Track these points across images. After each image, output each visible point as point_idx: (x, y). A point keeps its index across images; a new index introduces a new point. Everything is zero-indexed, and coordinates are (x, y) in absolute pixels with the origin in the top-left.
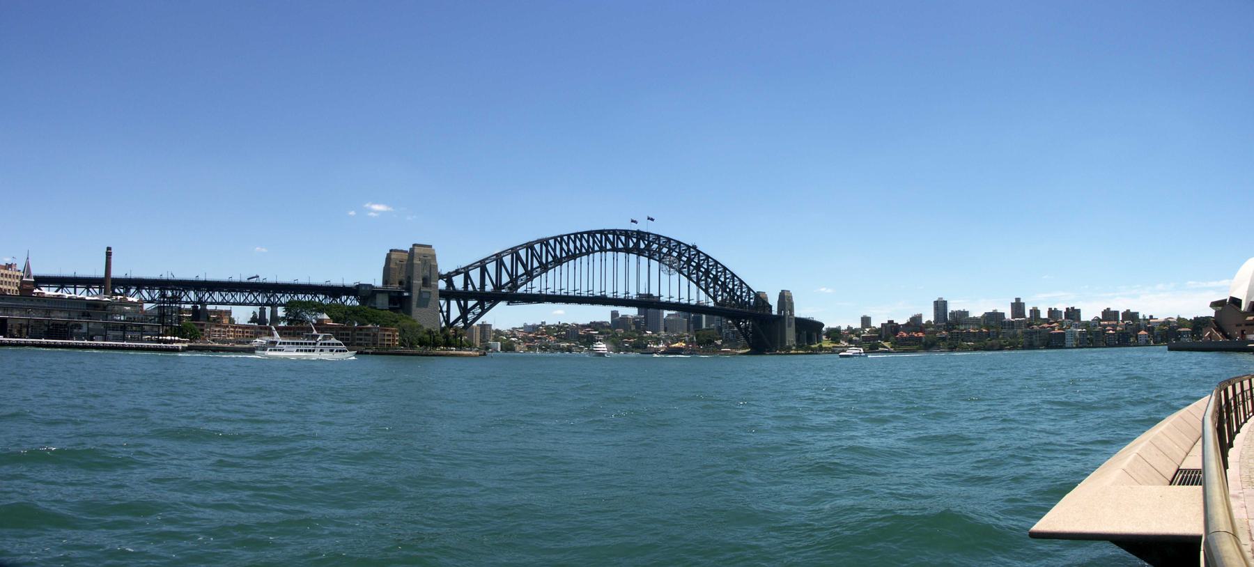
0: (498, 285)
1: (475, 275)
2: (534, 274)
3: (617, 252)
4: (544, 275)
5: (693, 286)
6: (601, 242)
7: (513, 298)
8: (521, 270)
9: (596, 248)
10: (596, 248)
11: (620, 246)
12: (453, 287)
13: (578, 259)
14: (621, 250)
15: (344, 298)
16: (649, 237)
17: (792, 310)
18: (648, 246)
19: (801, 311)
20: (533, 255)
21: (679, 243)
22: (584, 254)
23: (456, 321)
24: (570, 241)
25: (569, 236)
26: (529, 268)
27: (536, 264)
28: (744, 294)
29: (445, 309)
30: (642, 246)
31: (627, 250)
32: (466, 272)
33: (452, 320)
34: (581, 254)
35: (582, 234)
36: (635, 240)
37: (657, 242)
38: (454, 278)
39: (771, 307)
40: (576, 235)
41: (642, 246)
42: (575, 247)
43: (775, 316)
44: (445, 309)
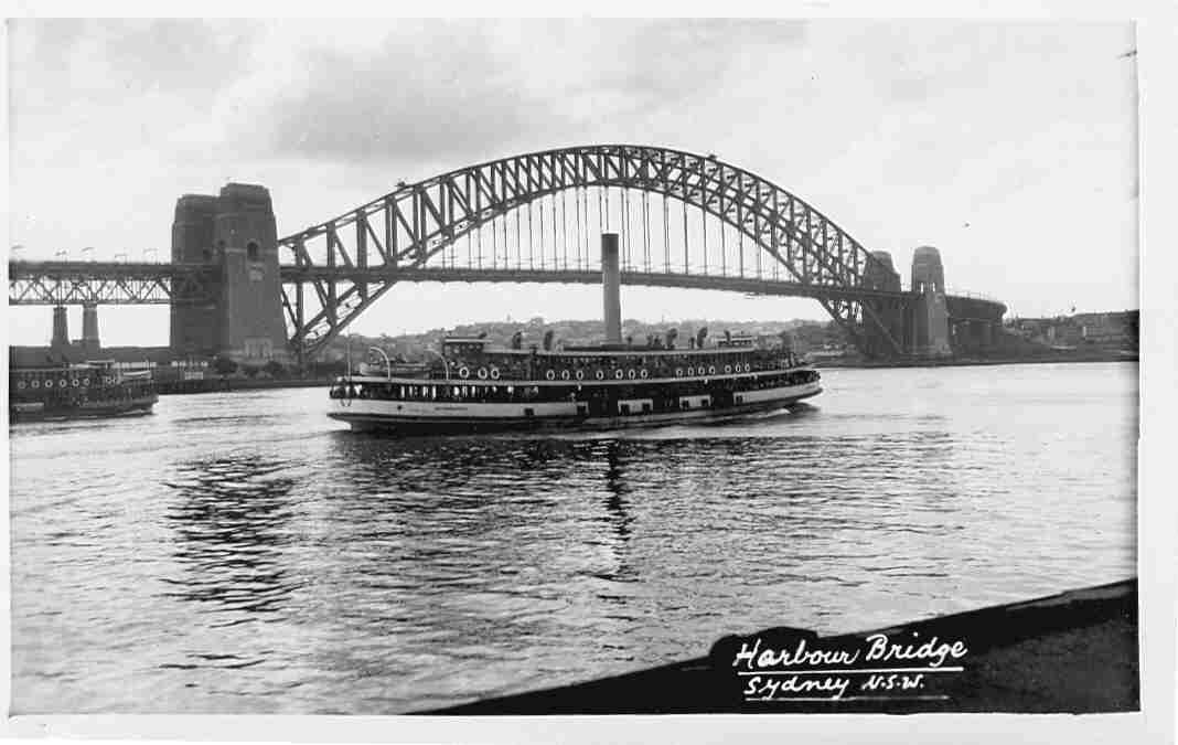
0: (391, 256)
1: (348, 235)
2: (457, 230)
4: (474, 232)
5: (748, 242)
6: (576, 169)
7: (417, 275)
8: (432, 225)
9: (568, 181)
10: (568, 181)
11: (612, 175)
12: (308, 260)
13: (535, 202)
14: (613, 183)
15: (96, 285)
16: (663, 157)
17: (939, 280)
18: (663, 176)
19: (959, 282)
22: (547, 192)
23: (316, 321)
24: (520, 168)
25: (517, 160)
26: (447, 222)
27: (459, 213)
28: (845, 255)
29: (292, 299)
30: (652, 173)
31: (627, 183)
32: (330, 229)
33: (306, 322)
34: (541, 193)
35: (541, 156)
36: (638, 163)
37: (679, 165)
38: (306, 243)
39: (897, 277)
40: (529, 157)
41: (652, 173)
42: (530, 180)
43: (906, 293)
44: (292, 299)
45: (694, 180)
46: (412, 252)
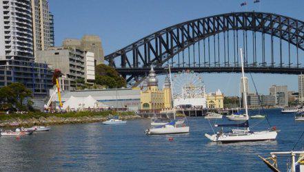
1: (130, 55)
2: (174, 52)
3: (237, 30)
4: (181, 53)
6: (224, 23)
8: (164, 50)
9: (220, 29)
10: (220, 29)
11: (240, 25)
13: (207, 39)
14: (241, 28)
18: (262, 24)
20: (172, 38)
21: (287, 18)
31: (245, 28)
32: (122, 53)
34: (209, 34)
36: (250, 19)
40: (204, 19)
41: (257, 24)
42: (204, 29)
45: (276, 25)
46: (155, 61)
